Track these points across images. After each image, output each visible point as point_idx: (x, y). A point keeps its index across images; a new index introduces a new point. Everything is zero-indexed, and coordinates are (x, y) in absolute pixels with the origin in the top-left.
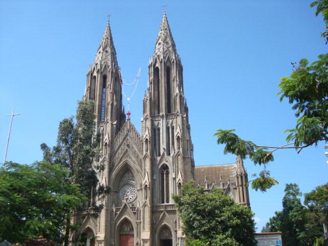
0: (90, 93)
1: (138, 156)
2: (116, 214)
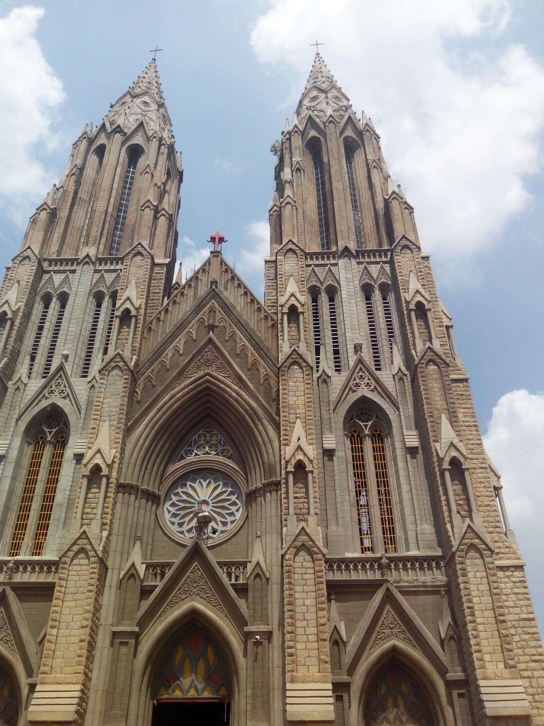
0: (78, 183)
1: (255, 363)
2: (145, 592)
